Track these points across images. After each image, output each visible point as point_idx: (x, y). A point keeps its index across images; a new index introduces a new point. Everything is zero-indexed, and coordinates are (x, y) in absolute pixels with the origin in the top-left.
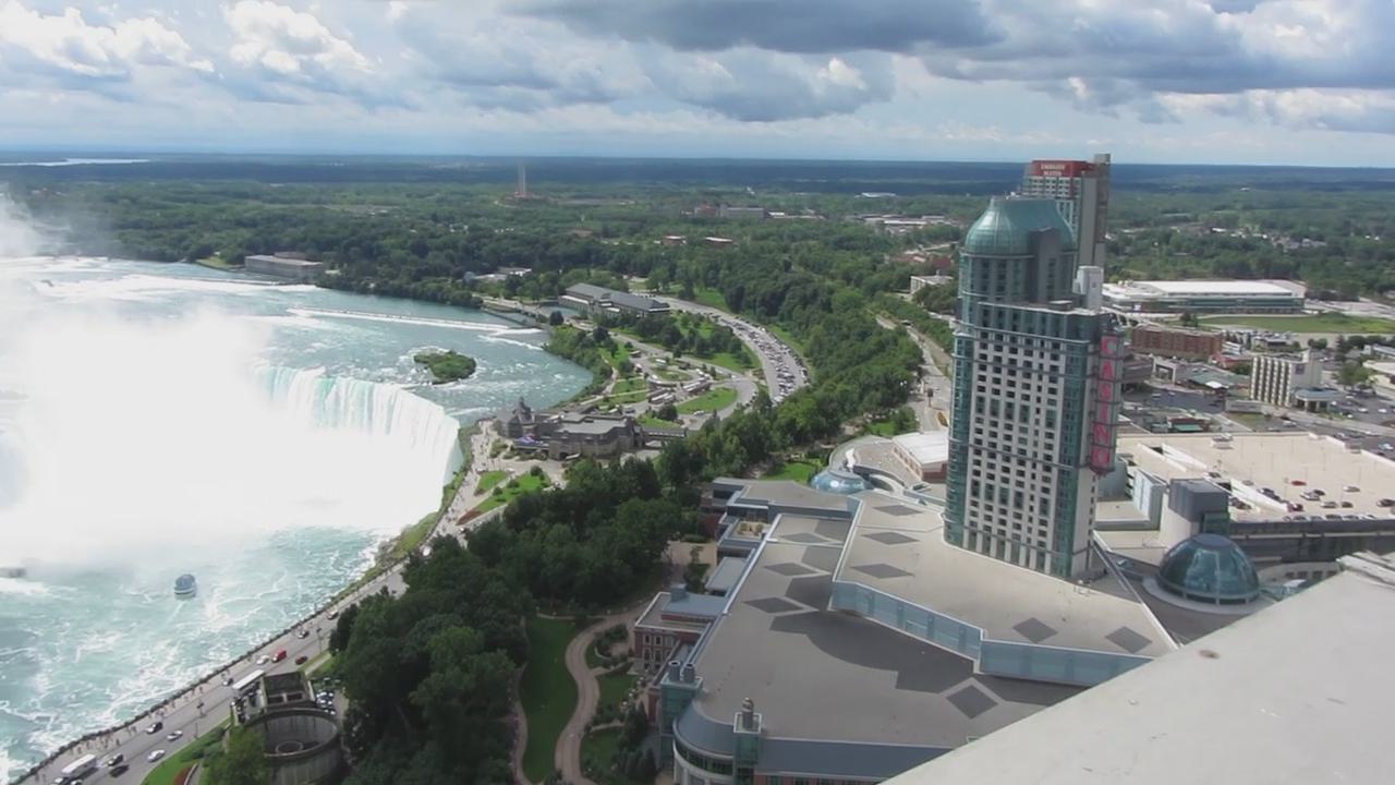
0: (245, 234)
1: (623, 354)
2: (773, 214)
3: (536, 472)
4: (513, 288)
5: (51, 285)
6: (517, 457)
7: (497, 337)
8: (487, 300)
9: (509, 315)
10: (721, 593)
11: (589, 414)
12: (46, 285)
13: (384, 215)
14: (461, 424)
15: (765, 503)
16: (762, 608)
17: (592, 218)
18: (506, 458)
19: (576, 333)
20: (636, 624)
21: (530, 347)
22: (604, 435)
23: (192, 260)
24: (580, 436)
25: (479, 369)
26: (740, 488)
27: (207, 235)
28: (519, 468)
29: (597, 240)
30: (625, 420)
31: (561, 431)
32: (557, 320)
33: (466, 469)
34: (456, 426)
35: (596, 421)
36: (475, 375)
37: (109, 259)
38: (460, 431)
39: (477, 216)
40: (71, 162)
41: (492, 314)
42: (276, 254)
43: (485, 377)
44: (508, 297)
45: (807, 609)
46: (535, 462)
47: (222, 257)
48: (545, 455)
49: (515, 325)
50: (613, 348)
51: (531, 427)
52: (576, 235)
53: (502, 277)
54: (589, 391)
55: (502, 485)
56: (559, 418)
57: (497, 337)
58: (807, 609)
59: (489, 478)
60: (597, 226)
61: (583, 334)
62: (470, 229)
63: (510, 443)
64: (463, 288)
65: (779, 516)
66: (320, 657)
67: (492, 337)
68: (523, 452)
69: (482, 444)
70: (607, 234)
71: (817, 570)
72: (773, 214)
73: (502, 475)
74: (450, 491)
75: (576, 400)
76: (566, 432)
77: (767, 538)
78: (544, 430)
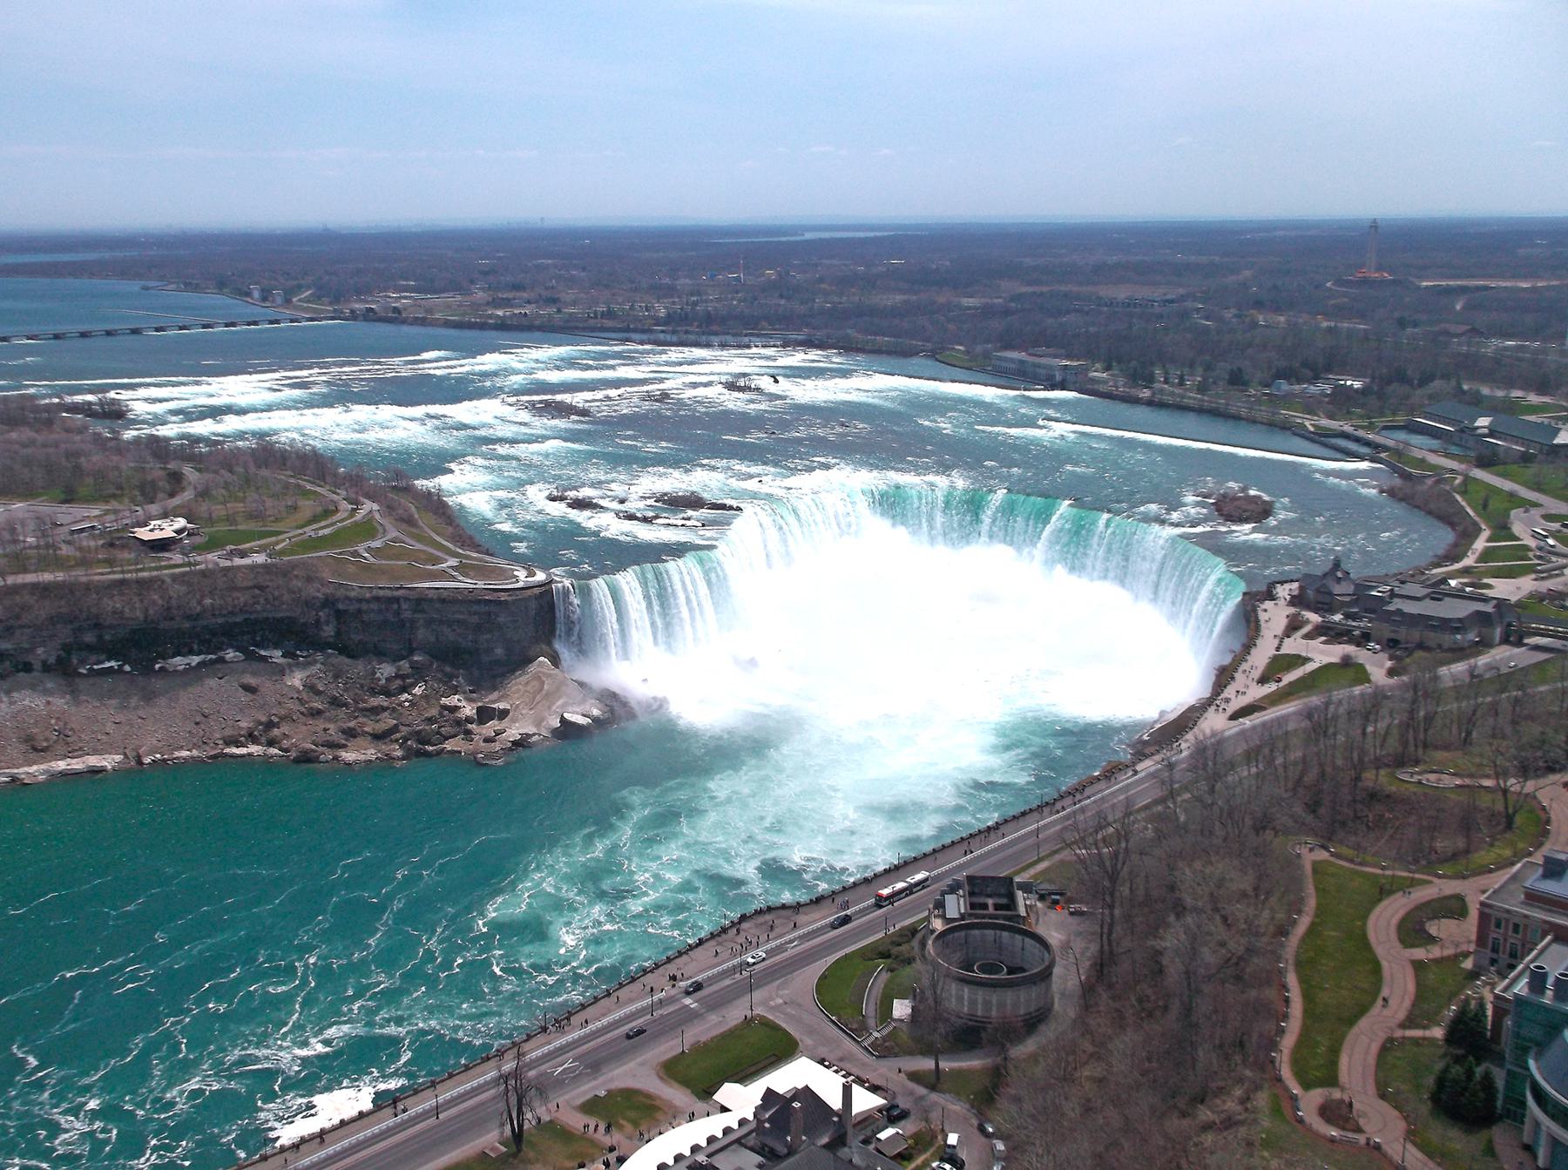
3: (1347, 662)
4: (1342, 402)
5: (776, 381)
6: (1324, 638)
9: (1334, 441)
11: (1438, 591)
18: (1307, 636)
20: (1482, 899)
22: (1460, 620)
28: (1323, 654)
30: (1495, 602)
31: (1391, 608)
33: (1248, 647)
35: (1447, 599)
36: (1272, 521)
38: (1245, 594)
40: (809, 236)
42: (1031, 351)
46: (1350, 649)
48: (1363, 640)
49: (1339, 456)
51: (1347, 599)
56: (1392, 590)
63: (1314, 618)
68: (1331, 633)
69: (1274, 616)
73: (1298, 660)
74: (1223, 677)
76: (1399, 610)
78: (1363, 602)
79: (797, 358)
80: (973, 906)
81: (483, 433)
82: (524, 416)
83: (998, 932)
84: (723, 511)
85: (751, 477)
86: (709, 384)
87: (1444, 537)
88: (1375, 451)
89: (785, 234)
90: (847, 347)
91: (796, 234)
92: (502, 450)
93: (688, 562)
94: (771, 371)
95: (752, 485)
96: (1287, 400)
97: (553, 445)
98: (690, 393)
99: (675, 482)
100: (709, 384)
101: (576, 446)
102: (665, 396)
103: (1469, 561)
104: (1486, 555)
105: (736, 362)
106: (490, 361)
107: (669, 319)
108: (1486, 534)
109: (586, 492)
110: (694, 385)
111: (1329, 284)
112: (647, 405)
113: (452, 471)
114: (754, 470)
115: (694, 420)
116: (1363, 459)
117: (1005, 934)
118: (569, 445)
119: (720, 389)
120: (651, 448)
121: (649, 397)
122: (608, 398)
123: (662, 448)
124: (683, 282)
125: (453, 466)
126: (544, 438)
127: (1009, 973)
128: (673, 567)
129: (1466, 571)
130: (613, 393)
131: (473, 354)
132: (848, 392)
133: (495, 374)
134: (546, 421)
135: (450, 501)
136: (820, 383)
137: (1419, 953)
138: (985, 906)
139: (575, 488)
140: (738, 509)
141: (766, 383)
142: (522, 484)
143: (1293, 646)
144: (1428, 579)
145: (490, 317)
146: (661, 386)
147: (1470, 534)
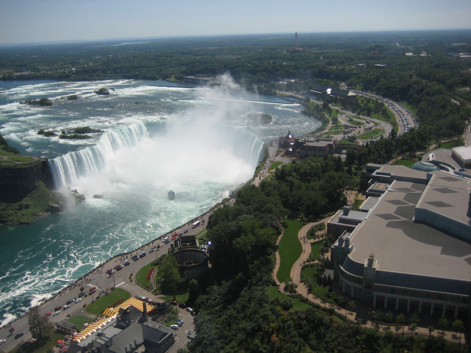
0: (184, 68)
1: (334, 114)
2: (407, 54)
4: (289, 87)
5: (114, 90)
7: (282, 107)
8: (277, 92)
9: (287, 98)
10: (367, 211)
12: (112, 90)
13: (238, 59)
14: (265, 142)
15: (389, 174)
16: (379, 216)
17: (325, 58)
18: (282, 156)
19: (315, 105)
21: (295, 111)
23: (164, 79)
24: (314, 148)
25: (274, 120)
26: (378, 168)
27: (170, 69)
29: (327, 66)
30: (333, 141)
31: (305, 145)
32: (308, 100)
34: (263, 143)
36: (272, 123)
37: (134, 80)
39: (276, 58)
40: (123, 44)
41: (281, 98)
42: (196, 75)
43: (276, 123)
44: (287, 91)
45: (403, 219)
47: (175, 77)
49: (289, 102)
50: (330, 111)
52: (318, 65)
53: (285, 83)
54: (319, 130)
55: (280, 167)
56: (305, 140)
57: (282, 107)
58: (403, 219)
59: (274, 164)
60: (327, 61)
61: (317, 106)
62: (273, 63)
64: (269, 87)
65: (395, 181)
66: (201, 231)
67: (281, 107)
69: (272, 151)
70: (330, 64)
71: (409, 203)
72: (407, 54)
73: (279, 163)
75: (313, 133)
76: (307, 146)
77: (389, 189)
79: (120, 82)
80: (183, 246)
81: (13, 113)
82: (28, 107)
83: (191, 252)
84: (99, 132)
85: (106, 121)
86: (91, 93)
87: (320, 124)
88: (299, 100)
89: (115, 44)
90: (136, 77)
91: (119, 44)
92: (20, 119)
93: (87, 149)
94: (111, 87)
95: (107, 124)
96: (273, 86)
97: (40, 116)
98: (84, 96)
99: (81, 124)
100: (91, 93)
101: (46, 116)
102: (74, 98)
103: (326, 131)
104: (331, 128)
105: (100, 85)
106: (14, 90)
107: (76, 73)
108: (331, 122)
109: (51, 130)
110: (86, 93)
111: (285, 52)
112: (70, 101)
113: (3, 128)
114: (108, 119)
115: (89, 104)
116: (293, 102)
117: (193, 253)
118: (43, 115)
119: (94, 94)
120: (72, 115)
121: (70, 98)
122: (57, 99)
123: (76, 114)
124: (82, 61)
125: (3, 126)
126: (36, 114)
127: (194, 264)
128: (81, 152)
129: (326, 133)
130: (59, 97)
131: (9, 88)
132: (137, 92)
133: (16, 94)
134: (36, 109)
135: (4, 137)
136: (127, 89)
137: (312, 241)
138: (187, 245)
139: (48, 129)
140: (103, 132)
141: (110, 91)
142: (27, 130)
143: (279, 159)
144: (315, 136)
145: (14, 76)
146: (75, 94)
147: (326, 122)
